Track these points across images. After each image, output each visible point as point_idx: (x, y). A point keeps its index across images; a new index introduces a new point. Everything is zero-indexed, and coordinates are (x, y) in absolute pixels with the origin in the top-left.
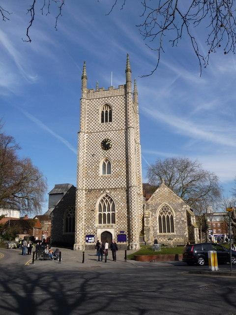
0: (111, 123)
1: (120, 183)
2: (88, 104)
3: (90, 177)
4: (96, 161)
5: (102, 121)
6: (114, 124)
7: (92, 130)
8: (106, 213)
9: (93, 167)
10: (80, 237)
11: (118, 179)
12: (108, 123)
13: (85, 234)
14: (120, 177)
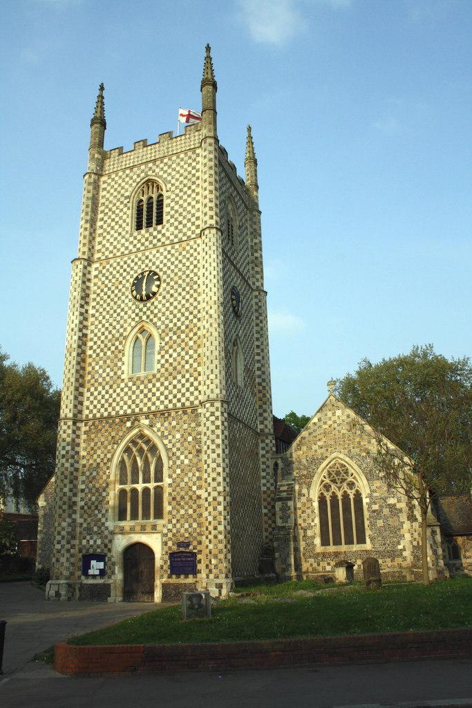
0: (159, 227)
1: (179, 396)
2: (105, 186)
3: (100, 384)
4: (117, 335)
5: (139, 227)
6: (168, 229)
7: (111, 252)
8: (140, 487)
9: (109, 353)
10: (63, 560)
11: (175, 382)
12: (151, 229)
13: (80, 551)
14: (179, 377)
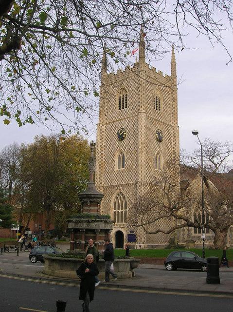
8: (120, 210)
